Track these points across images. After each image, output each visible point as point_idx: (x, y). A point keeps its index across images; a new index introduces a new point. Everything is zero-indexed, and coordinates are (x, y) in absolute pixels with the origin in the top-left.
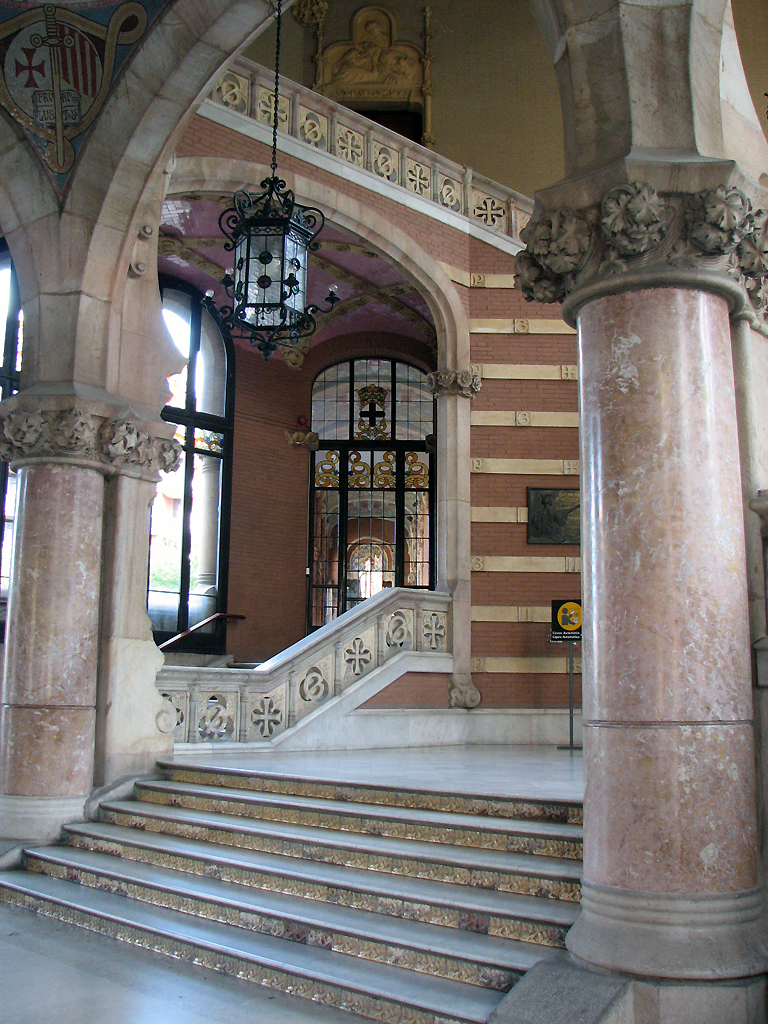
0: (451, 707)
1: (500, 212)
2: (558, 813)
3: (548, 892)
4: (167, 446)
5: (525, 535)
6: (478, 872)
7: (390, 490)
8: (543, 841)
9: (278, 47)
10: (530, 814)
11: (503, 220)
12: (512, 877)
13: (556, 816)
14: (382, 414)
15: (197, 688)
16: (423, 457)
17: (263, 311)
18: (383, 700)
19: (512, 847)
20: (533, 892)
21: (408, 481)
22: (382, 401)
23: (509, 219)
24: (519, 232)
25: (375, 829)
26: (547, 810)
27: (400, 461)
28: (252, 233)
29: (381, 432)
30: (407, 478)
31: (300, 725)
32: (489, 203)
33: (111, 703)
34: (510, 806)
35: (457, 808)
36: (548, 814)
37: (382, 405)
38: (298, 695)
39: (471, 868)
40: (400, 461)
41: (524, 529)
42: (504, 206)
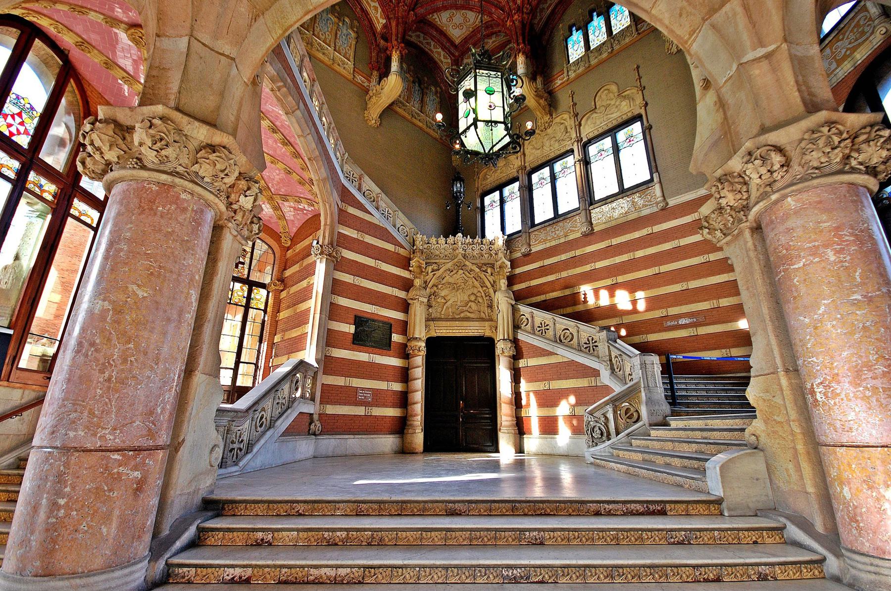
0: (309, 434)
2: (659, 508)
3: (766, 575)
4: (255, 220)
6: (703, 569)
7: (242, 306)
8: (698, 533)
9: (204, 44)
10: (637, 511)
12: (706, 568)
13: (658, 510)
14: (243, 263)
15: (234, 423)
16: (263, 292)
17: (491, 125)
18: (290, 432)
19: (672, 540)
20: (755, 577)
21: (253, 304)
22: (244, 256)
23: (360, 185)
25: (536, 539)
26: (651, 507)
27: (250, 292)
28: (478, 74)
29: (241, 273)
30: (252, 301)
31: (255, 450)
32: (352, 173)
33: (183, 440)
34: (620, 506)
35: (573, 511)
36: (651, 510)
37: (244, 259)
38: (253, 427)
39: (695, 567)
40: (250, 292)
41: (351, 336)
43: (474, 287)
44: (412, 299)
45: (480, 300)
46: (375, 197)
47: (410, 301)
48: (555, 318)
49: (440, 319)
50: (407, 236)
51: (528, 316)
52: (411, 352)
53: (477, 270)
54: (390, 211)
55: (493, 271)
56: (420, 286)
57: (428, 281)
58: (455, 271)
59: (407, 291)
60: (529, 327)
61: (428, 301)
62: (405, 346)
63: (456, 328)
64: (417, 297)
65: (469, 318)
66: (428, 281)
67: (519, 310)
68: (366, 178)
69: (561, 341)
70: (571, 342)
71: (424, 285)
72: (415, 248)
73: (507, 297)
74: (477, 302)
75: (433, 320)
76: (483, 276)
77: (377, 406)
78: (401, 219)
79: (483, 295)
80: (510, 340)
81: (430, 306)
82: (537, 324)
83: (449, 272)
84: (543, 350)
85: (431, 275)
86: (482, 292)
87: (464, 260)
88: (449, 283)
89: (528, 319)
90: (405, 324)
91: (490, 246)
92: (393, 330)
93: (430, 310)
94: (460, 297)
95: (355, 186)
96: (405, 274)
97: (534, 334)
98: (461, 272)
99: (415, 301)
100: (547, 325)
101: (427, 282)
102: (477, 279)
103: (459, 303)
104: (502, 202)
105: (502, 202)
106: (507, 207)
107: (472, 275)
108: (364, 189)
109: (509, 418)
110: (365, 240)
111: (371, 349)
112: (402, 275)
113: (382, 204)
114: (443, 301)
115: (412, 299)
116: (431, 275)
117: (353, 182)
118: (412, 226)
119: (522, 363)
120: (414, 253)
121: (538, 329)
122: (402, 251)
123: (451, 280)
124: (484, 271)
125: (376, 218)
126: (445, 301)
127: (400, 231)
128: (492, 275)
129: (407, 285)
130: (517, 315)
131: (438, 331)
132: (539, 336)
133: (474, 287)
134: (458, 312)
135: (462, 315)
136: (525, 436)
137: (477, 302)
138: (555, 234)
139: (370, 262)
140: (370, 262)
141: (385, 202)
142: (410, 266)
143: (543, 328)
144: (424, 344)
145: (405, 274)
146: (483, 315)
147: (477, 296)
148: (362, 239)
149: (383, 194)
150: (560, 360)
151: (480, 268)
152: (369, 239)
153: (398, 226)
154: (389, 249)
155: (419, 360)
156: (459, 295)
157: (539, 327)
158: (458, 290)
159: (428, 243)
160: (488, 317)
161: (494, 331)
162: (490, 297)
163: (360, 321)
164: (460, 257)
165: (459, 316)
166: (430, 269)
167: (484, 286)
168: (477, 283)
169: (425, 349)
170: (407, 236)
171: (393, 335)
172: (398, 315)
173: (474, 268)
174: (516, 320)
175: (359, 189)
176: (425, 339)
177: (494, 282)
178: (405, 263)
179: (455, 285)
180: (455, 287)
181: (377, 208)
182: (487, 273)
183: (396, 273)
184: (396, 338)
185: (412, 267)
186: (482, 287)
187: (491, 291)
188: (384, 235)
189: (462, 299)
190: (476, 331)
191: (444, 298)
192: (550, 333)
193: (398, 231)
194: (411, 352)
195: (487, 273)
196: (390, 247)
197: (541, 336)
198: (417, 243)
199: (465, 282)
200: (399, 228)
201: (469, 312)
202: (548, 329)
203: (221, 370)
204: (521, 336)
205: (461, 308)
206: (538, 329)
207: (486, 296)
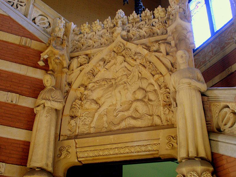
45: (152, 96)
53: (146, 52)
57: (73, 80)
65: (134, 128)
73: (189, 78)
74: (146, 100)
79: (156, 87)
80: (202, 159)
85: (77, 71)
87: (125, 42)
88: (105, 80)
90: (26, 147)
96: (36, 74)
103: (118, 107)
114: (94, 106)
122: (34, 45)
123: (109, 75)
128: (167, 54)
130: (215, 110)
131: (80, 155)
133: (141, 78)
134: (116, 121)
135: (123, 125)
137: (146, 100)
145: (36, 74)
146: (157, 121)
151: (148, 48)
156: (118, 94)
158: (117, 86)
160: (165, 123)
164: (119, 39)
165: (117, 127)
168: (146, 73)
179: (113, 81)
182: (161, 52)
189: (124, 99)
195: (161, 52)
201: (134, 118)
205: (121, 114)
207: (160, 88)
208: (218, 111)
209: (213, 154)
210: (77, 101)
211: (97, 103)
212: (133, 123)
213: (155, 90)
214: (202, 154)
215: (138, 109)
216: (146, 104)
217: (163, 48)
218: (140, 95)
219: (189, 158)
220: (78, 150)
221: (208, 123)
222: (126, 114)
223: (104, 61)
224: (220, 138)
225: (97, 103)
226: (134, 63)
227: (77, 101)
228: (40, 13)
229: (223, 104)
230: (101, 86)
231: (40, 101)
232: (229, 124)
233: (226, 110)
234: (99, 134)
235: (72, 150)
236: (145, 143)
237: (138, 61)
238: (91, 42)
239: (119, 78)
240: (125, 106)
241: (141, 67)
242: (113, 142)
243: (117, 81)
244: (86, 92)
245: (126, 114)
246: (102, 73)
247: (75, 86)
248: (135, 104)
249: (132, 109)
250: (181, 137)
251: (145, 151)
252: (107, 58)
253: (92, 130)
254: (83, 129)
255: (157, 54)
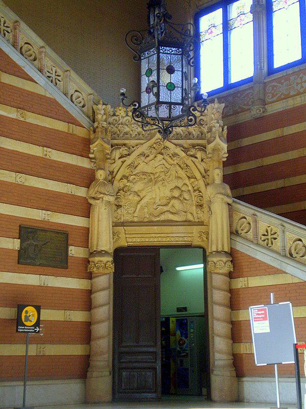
1: (9, 30)
5: (17, 258)
11: (11, 36)
23: (15, 37)
24: (20, 47)
42: (11, 25)
43: (178, 178)
44: (94, 198)
45: (186, 196)
46: (37, 52)
47: (91, 201)
48: (285, 224)
49: (132, 224)
50: (83, 106)
51: (249, 219)
52: (95, 269)
53: (183, 154)
54: (60, 72)
55: (204, 156)
56: (105, 179)
57: (116, 171)
58: (152, 157)
59: (88, 187)
60: (250, 235)
61: (116, 199)
62: (87, 262)
63: (153, 235)
64: (102, 195)
65: (172, 221)
66: (116, 171)
67: (238, 211)
68: (23, 25)
69: (291, 255)
70: (302, 258)
71: (110, 178)
72: (96, 125)
75: (123, 224)
76: (189, 162)
77: (52, 342)
78: (75, 83)
79: (190, 188)
81: (119, 206)
82: (262, 231)
83: (143, 158)
84: (268, 266)
85: (119, 162)
86: (188, 184)
88: (144, 173)
89: (249, 224)
90: (87, 231)
91: (202, 117)
92: (70, 242)
93: (119, 211)
94: (161, 192)
95: (8, 41)
96: (84, 163)
97: (258, 244)
98: (160, 157)
99: (98, 201)
100: (275, 233)
101: (113, 172)
102: (182, 166)
104: (227, 27)
105: (227, 27)
106: (234, 36)
107: (176, 161)
108: (21, 43)
109: (225, 357)
110: (27, 121)
111: (41, 269)
112: (80, 164)
113: (47, 63)
114: (137, 199)
115: (94, 198)
116: (119, 162)
117: (4, 34)
118: (90, 90)
119: (240, 283)
120: (94, 132)
121: (263, 238)
122: (80, 132)
123: (148, 169)
124: (191, 156)
125: (41, 86)
126: (137, 199)
127: (74, 99)
128: (202, 160)
129: (88, 179)
130: (236, 217)
132: (263, 247)
133: (178, 178)
134: (156, 212)
135: (162, 218)
136: (245, 379)
137: (182, 199)
138: (302, 87)
139: (36, 151)
140: (36, 151)
141: (51, 60)
142: (89, 153)
143: (269, 237)
144: (111, 259)
145: (84, 163)
146: (190, 218)
147: (182, 191)
148: (22, 119)
149: (47, 47)
150: (289, 280)
151: (186, 150)
152: (33, 119)
153: (71, 92)
154: (60, 129)
155: (104, 281)
156: (157, 190)
157: (264, 235)
158: (156, 182)
159: (114, 115)
161: (205, 239)
162: (200, 192)
163: (26, 231)
165: (158, 219)
166: (117, 154)
167: (192, 178)
168: (182, 173)
169: (112, 266)
170: (83, 106)
171: (71, 248)
172: (77, 221)
173: (178, 150)
174: (235, 224)
175: (14, 45)
176: (112, 251)
177: (206, 171)
178: (83, 147)
179: (152, 176)
180: (151, 179)
181: (41, 70)
182: (196, 158)
183: (71, 163)
184: (75, 252)
185: (93, 153)
186: (189, 177)
187: (201, 184)
188: (50, 108)
190: (181, 239)
191: (137, 194)
192: (278, 245)
193: (72, 100)
194: (95, 269)
195: (196, 158)
196: (61, 126)
197: (268, 247)
198: (99, 117)
199: (166, 172)
200: (72, 95)
201: (172, 213)
202: (275, 239)
203: (25, 345)
204: (242, 246)
205: (160, 207)
206: (263, 238)
207: (195, 191)
208: (238, 219)
209: (231, 248)
210: (121, 192)
211: (139, 196)
212: (171, 217)
213: (189, 191)
214: (226, 249)
215: (175, 205)
216: (182, 202)
217: (199, 155)
218: (176, 193)
219: (217, 252)
220: (127, 236)
221: (231, 226)
222: (165, 208)
223: (143, 154)
224: (238, 239)
225: (139, 196)
226: (172, 162)
227: (121, 192)
228: (76, 88)
229: (242, 215)
230: (141, 179)
231: (92, 192)
232: (245, 231)
233: (244, 220)
234: (141, 223)
235: (122, 235)
236: (182, 235)
237: (175, 162)
238: (127, 129)
239: (158, 174)
240: (164, 201)
241: (177, 166)
242: (157, 232)
243: (156, 176)
244: (128, 184)
245: (165, 208)
246: (142, 167)
247: (118, 177)
248: (174, 202)
249: (170, 205)
250: (213, 236)
251: (182, 241)
252: (147, 152)
253: (136, 220)
254: (128, 218)
255: (193, 159)
